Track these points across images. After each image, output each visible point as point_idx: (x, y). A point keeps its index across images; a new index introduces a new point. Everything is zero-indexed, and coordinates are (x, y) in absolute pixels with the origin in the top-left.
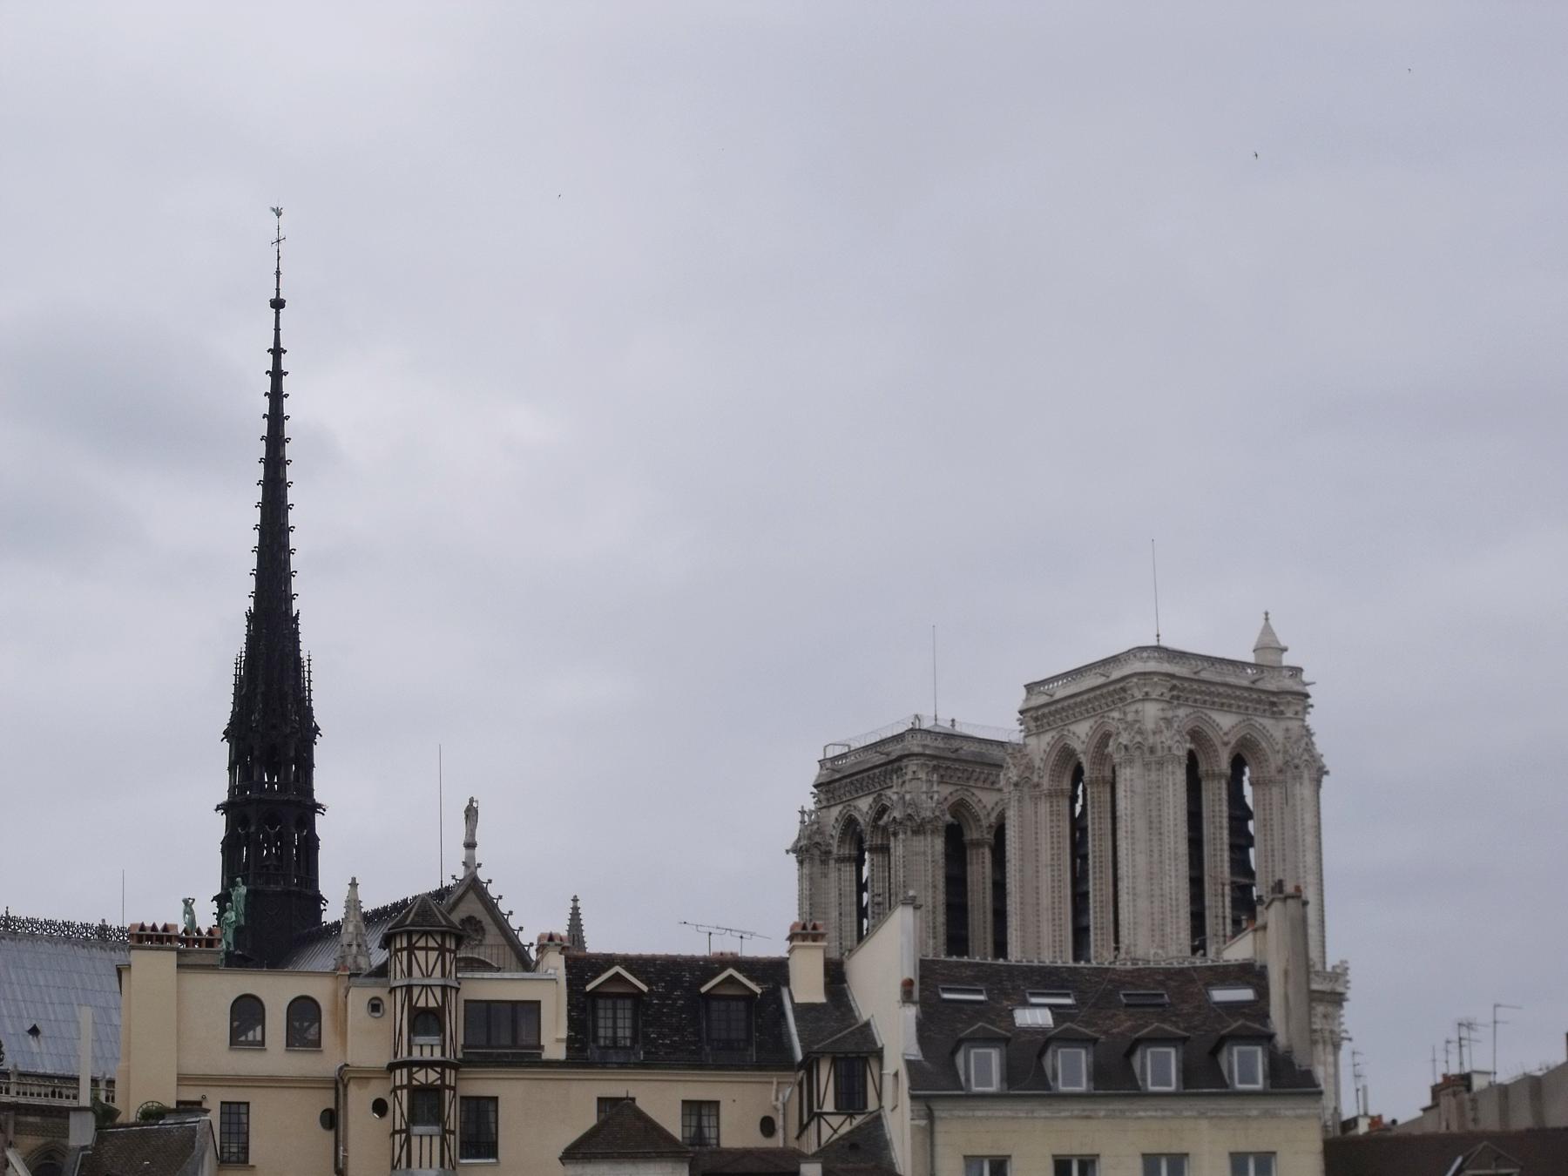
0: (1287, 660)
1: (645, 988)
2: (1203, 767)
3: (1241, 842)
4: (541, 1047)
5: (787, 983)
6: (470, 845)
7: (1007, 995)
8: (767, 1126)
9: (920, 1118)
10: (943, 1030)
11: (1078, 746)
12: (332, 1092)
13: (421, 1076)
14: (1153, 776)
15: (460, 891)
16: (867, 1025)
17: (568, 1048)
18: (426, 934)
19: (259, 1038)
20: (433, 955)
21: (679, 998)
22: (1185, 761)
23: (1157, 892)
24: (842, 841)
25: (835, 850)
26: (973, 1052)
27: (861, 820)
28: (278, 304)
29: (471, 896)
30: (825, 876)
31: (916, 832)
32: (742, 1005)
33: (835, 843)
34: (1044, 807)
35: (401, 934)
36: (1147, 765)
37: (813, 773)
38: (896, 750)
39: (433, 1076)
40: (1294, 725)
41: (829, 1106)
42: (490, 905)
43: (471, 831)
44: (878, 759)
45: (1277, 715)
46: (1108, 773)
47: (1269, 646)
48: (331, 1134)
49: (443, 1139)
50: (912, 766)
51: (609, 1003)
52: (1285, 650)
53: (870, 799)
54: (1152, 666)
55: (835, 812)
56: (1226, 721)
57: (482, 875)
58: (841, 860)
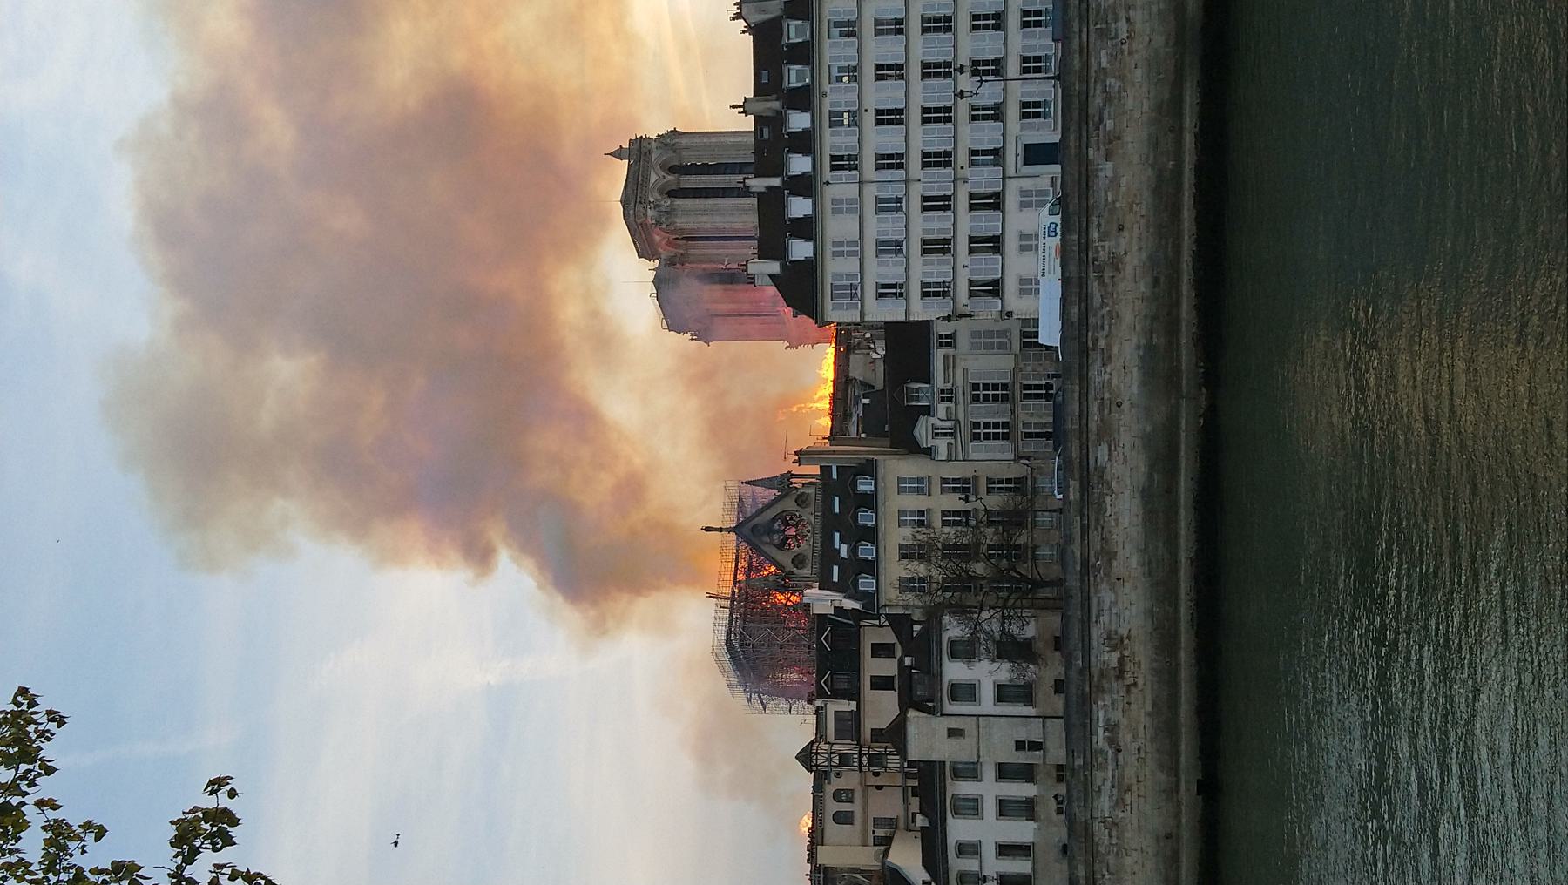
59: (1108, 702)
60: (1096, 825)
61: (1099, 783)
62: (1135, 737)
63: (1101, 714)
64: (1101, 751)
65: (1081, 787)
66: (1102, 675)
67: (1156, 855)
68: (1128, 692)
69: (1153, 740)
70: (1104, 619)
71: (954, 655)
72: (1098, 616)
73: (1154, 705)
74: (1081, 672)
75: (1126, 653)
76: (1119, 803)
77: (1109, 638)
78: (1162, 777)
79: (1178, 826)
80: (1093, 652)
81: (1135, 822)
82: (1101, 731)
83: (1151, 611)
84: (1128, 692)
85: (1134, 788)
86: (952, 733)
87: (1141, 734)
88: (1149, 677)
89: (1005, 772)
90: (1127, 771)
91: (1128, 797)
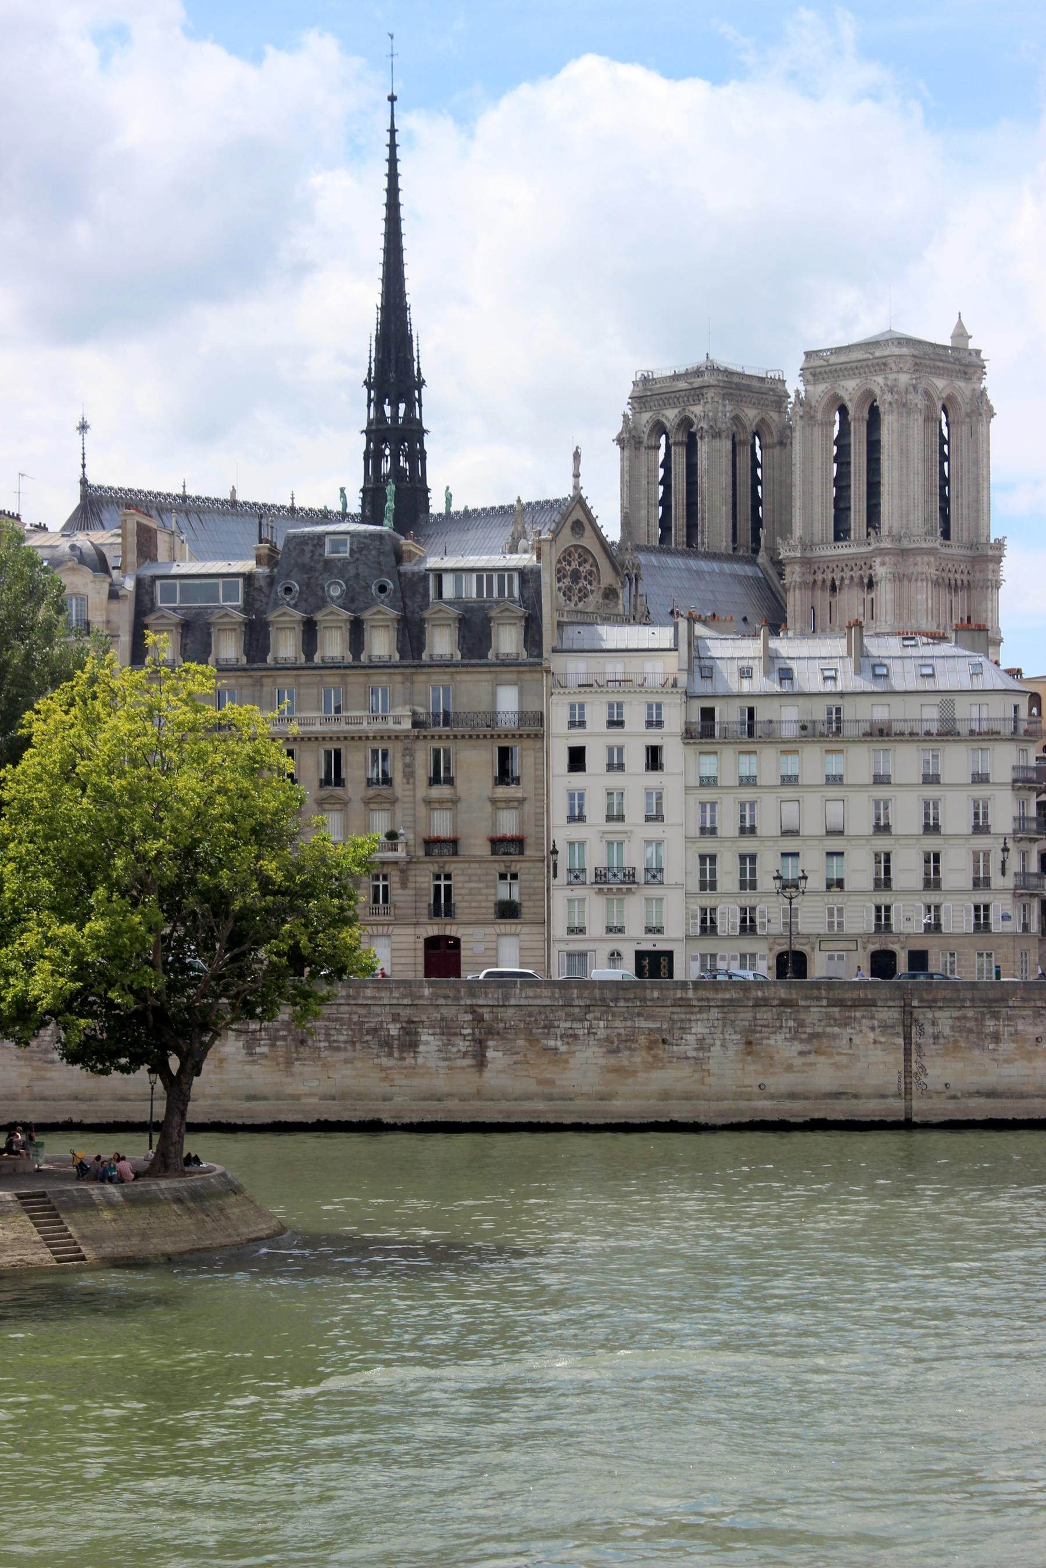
6: (577, 476)
11: (846, 398)
14: (904, 421)
24: (650, 435)
27: (668, 425)
28: (392, 99)
30: (637, 457)
33: (645, 437)
34: (817, 431)
36: (900, 414)
37: (628, 389)
38: (698, 382)
42: (587, 512)
44: (682, 385)
47: (961, 333)
50: (710, 394)
53: (676, 411)
54: (905, 351)
55: (646, 416)
56: (940, 383)
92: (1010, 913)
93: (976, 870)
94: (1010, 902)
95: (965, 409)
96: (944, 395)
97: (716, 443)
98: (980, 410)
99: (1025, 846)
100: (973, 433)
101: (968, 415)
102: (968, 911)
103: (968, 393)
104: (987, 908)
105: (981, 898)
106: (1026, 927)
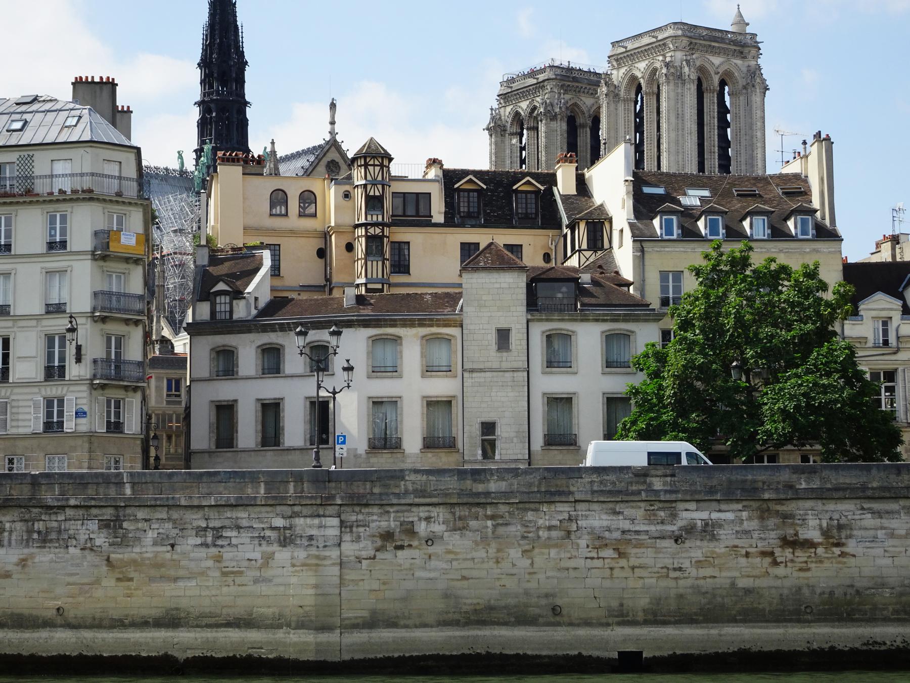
0: (749, 30)
1: (485, 187)
2: (705, 86)
3: (724, 124)
4: (431, 217)
5: (556, 185)
6: (333, 123)
7: (676, 190)
8: (547, 257)
9: (637, 251)
10: (644, 206)
11: (639, 75)
12: (323, 240)
13: (372, 231)
15: (327, 147)
16: (602, 205)
17: (445, 218)
18: (374, 157)
19: (283, 212)
20: (377, 168)
21: (501, 192)
22: (696, 82)
23: (680, 151)
24: (512, 124)
25: (508, 128)
26: (664, 217)
29: (333, 149)
30: (503, 142)
31: (551, 120)
32: (533, 196)
33: (509, 125)
34: (621, 107)
35: (360, 157)
36: (676, 85)
37: (497, 89)
39: (378, 231)
40: (753, 63)
41: (584, 246)
43: (333, 117)
45: (743, 57)
46: (656, 90)
47: (741, 21)
48: (322, 261)
49: (383, 263)
51: (466, 194)
52: (748, 24)
53: (528, 102)
55: (509, 109)
56: (717, 60)
57: (339, 138)
58: (512, 134)
59: (746, 525)
60: (565, 508)
61: (628, 512)
62: (699, 564)
63: (730, 516)
64: (674, 516)
65: (620, 486)
66: (785, 516)
67: (527, 593)
68: (764, 554)
69: (697, 590)
70: (869, 520)
71: (610, 338)
72: (873, 512)
73: (748, 591)
74: (791, 487)
75: (820, 550)
76: (599, 541)
77: (840, 527)
78: (644, 602)
79: (571, 624)
80: (819, 505)
81: (572, 564)
82: (704, 515)
83: (883, 585)
84: (764, 554)
85: (623, 562)
86: (503, 335)
87: (703, 572)
88: (787, 583)
89: (438, 406)
90: (650, 552)
91: (608, 553)
92: (86, 408)
93: (50, 356)
94: (85, 395)
95: (742, 82)
96: (721, 71)
97: (554, 125)
98: (755, 82)
99: (115, 328)
100: (748, 103)
101: (745, 87)
102: (36, 407)
103: (744, 69)
104: (61, 402)
105: (54, 390)
106: (115, 427)
